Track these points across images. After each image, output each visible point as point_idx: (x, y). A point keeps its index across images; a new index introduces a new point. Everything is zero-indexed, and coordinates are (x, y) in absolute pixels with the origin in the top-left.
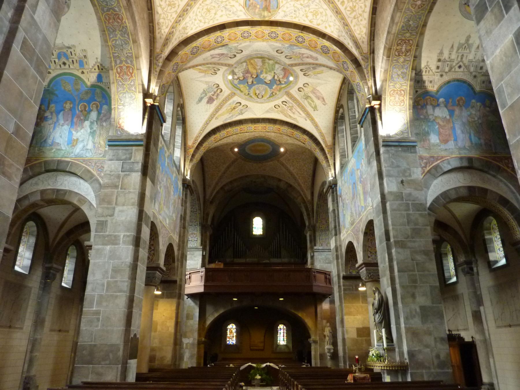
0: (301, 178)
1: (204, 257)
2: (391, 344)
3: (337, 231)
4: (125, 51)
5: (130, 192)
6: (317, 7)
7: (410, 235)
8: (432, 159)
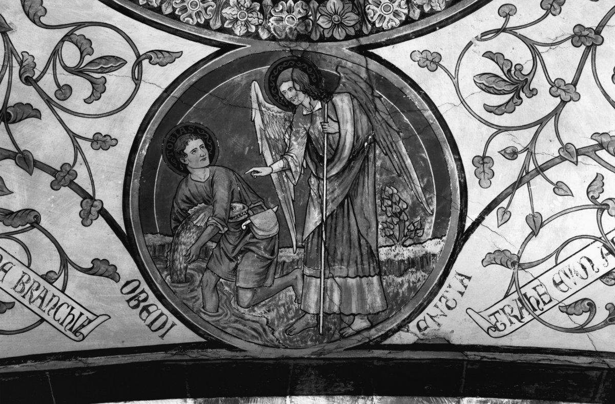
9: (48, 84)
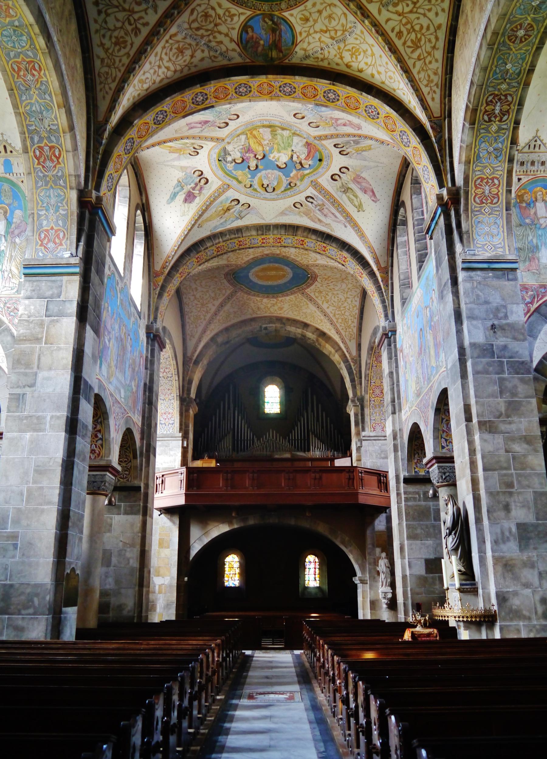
0: (340, 321)
1: (185, 450)
2: (472, 582)
3: (396, 407)
4: (46, 122)
5: (59, 349)
6: (358, 42)
7: (503, 412)
8: (543, 291)
9: (223, 19)
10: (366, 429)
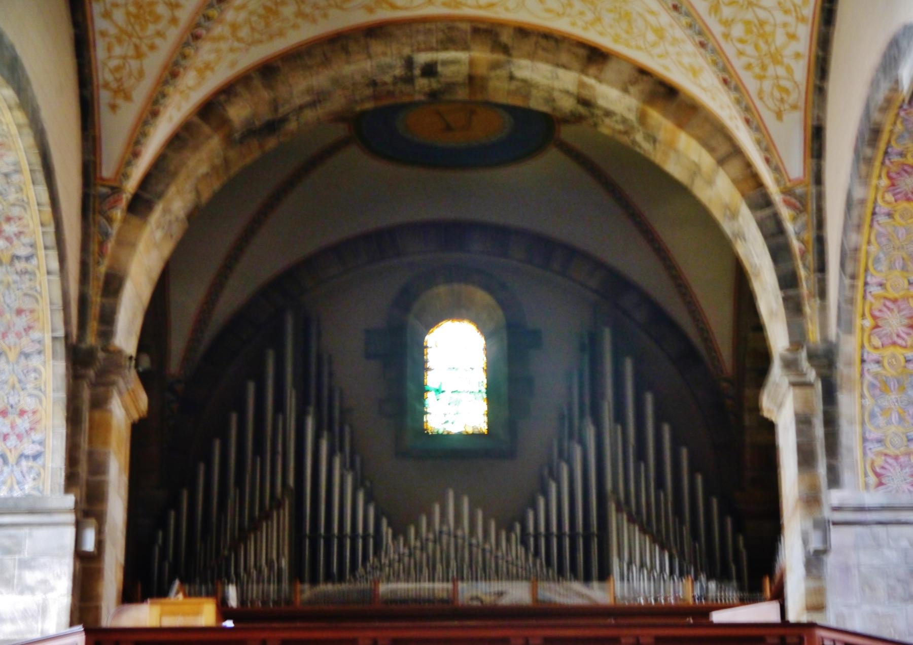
0: (737, 31)
1: (87, 569)
10: (846, 476)
